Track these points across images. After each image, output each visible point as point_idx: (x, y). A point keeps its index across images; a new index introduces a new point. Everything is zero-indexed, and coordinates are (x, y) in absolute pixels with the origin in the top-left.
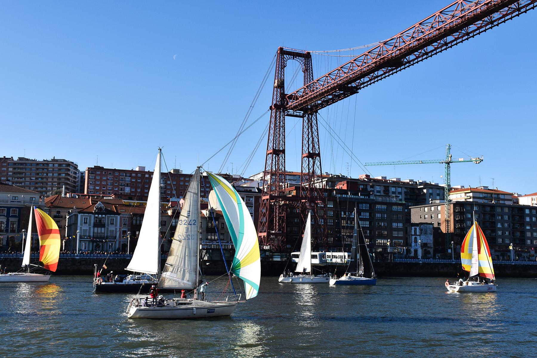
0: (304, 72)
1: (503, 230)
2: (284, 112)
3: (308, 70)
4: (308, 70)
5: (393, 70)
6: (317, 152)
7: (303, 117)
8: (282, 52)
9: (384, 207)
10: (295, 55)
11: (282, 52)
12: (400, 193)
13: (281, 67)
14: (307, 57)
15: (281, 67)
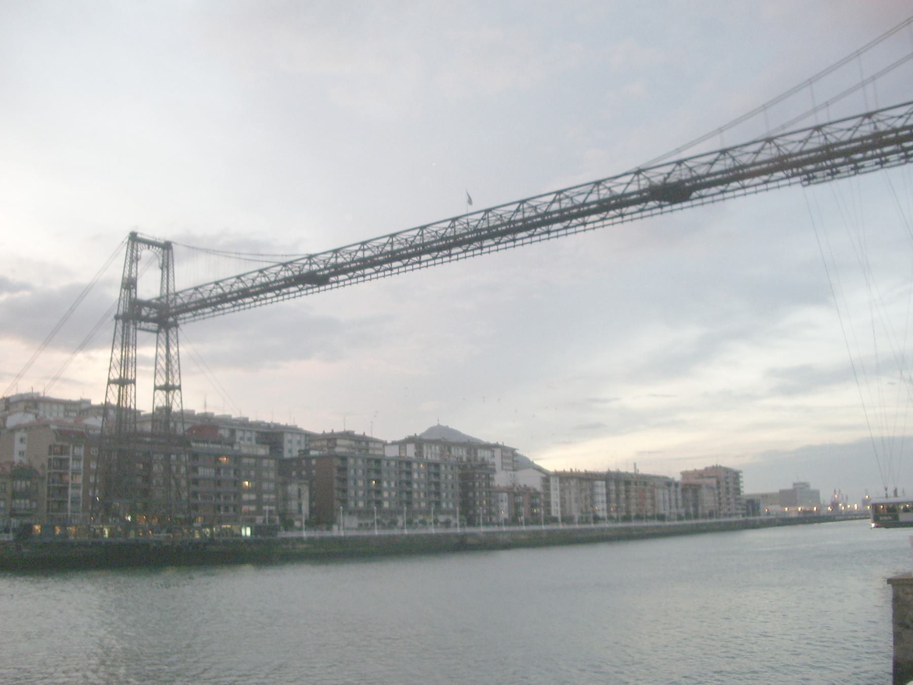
0: (162, 269)
1: (389, 490)
2: (136, 324)
3: (166, 266)
4: (166, 266)
5: (312, 288)
6: (177, 384)
7: (158, 332)
8: (134, 238)
9: (252, 461)
10: (150, 243)
11: (134, 238)
12: (249, 439)
13: (134, 259)
14: (167, 247)
15: (134, 259)
